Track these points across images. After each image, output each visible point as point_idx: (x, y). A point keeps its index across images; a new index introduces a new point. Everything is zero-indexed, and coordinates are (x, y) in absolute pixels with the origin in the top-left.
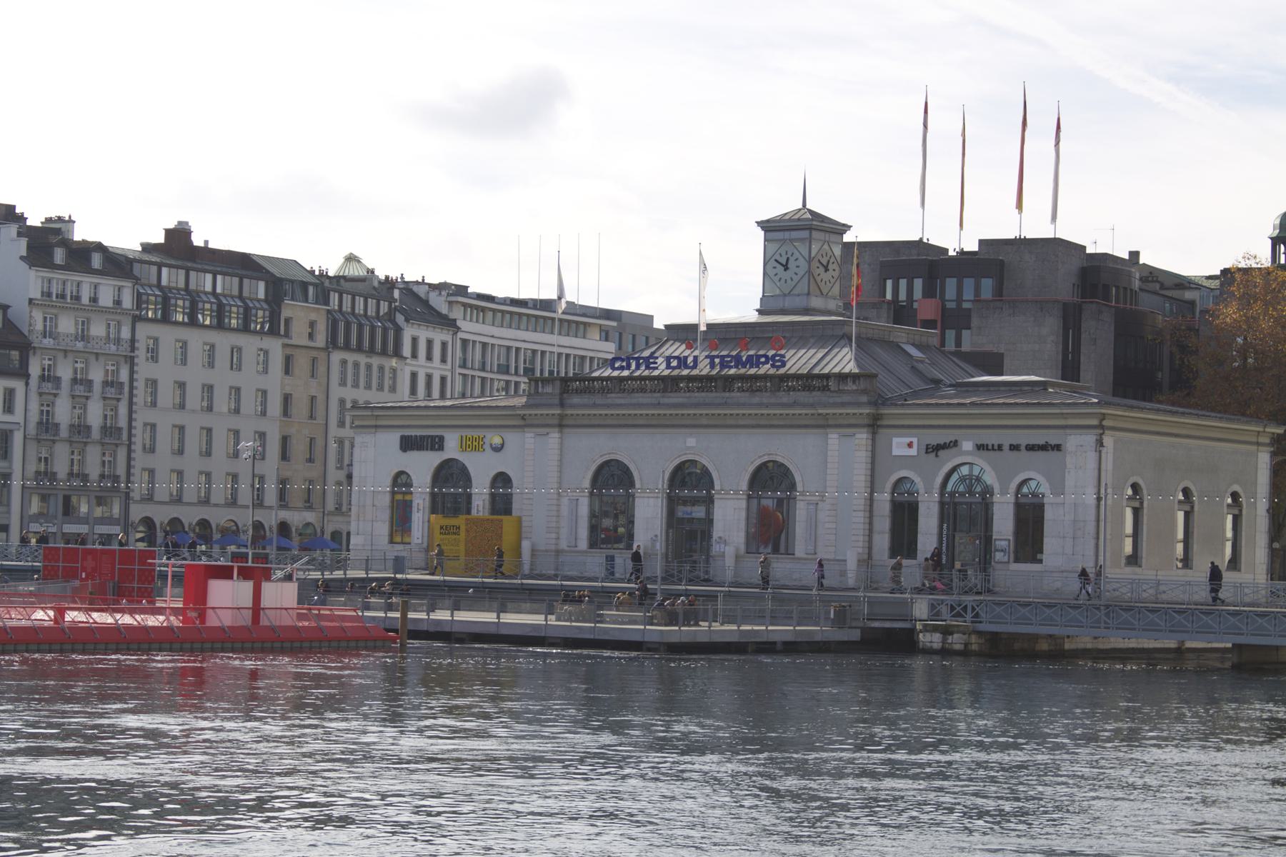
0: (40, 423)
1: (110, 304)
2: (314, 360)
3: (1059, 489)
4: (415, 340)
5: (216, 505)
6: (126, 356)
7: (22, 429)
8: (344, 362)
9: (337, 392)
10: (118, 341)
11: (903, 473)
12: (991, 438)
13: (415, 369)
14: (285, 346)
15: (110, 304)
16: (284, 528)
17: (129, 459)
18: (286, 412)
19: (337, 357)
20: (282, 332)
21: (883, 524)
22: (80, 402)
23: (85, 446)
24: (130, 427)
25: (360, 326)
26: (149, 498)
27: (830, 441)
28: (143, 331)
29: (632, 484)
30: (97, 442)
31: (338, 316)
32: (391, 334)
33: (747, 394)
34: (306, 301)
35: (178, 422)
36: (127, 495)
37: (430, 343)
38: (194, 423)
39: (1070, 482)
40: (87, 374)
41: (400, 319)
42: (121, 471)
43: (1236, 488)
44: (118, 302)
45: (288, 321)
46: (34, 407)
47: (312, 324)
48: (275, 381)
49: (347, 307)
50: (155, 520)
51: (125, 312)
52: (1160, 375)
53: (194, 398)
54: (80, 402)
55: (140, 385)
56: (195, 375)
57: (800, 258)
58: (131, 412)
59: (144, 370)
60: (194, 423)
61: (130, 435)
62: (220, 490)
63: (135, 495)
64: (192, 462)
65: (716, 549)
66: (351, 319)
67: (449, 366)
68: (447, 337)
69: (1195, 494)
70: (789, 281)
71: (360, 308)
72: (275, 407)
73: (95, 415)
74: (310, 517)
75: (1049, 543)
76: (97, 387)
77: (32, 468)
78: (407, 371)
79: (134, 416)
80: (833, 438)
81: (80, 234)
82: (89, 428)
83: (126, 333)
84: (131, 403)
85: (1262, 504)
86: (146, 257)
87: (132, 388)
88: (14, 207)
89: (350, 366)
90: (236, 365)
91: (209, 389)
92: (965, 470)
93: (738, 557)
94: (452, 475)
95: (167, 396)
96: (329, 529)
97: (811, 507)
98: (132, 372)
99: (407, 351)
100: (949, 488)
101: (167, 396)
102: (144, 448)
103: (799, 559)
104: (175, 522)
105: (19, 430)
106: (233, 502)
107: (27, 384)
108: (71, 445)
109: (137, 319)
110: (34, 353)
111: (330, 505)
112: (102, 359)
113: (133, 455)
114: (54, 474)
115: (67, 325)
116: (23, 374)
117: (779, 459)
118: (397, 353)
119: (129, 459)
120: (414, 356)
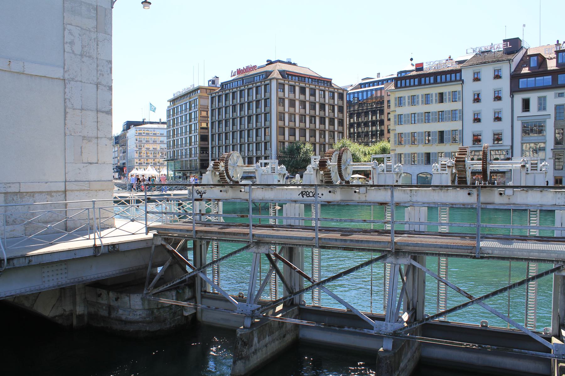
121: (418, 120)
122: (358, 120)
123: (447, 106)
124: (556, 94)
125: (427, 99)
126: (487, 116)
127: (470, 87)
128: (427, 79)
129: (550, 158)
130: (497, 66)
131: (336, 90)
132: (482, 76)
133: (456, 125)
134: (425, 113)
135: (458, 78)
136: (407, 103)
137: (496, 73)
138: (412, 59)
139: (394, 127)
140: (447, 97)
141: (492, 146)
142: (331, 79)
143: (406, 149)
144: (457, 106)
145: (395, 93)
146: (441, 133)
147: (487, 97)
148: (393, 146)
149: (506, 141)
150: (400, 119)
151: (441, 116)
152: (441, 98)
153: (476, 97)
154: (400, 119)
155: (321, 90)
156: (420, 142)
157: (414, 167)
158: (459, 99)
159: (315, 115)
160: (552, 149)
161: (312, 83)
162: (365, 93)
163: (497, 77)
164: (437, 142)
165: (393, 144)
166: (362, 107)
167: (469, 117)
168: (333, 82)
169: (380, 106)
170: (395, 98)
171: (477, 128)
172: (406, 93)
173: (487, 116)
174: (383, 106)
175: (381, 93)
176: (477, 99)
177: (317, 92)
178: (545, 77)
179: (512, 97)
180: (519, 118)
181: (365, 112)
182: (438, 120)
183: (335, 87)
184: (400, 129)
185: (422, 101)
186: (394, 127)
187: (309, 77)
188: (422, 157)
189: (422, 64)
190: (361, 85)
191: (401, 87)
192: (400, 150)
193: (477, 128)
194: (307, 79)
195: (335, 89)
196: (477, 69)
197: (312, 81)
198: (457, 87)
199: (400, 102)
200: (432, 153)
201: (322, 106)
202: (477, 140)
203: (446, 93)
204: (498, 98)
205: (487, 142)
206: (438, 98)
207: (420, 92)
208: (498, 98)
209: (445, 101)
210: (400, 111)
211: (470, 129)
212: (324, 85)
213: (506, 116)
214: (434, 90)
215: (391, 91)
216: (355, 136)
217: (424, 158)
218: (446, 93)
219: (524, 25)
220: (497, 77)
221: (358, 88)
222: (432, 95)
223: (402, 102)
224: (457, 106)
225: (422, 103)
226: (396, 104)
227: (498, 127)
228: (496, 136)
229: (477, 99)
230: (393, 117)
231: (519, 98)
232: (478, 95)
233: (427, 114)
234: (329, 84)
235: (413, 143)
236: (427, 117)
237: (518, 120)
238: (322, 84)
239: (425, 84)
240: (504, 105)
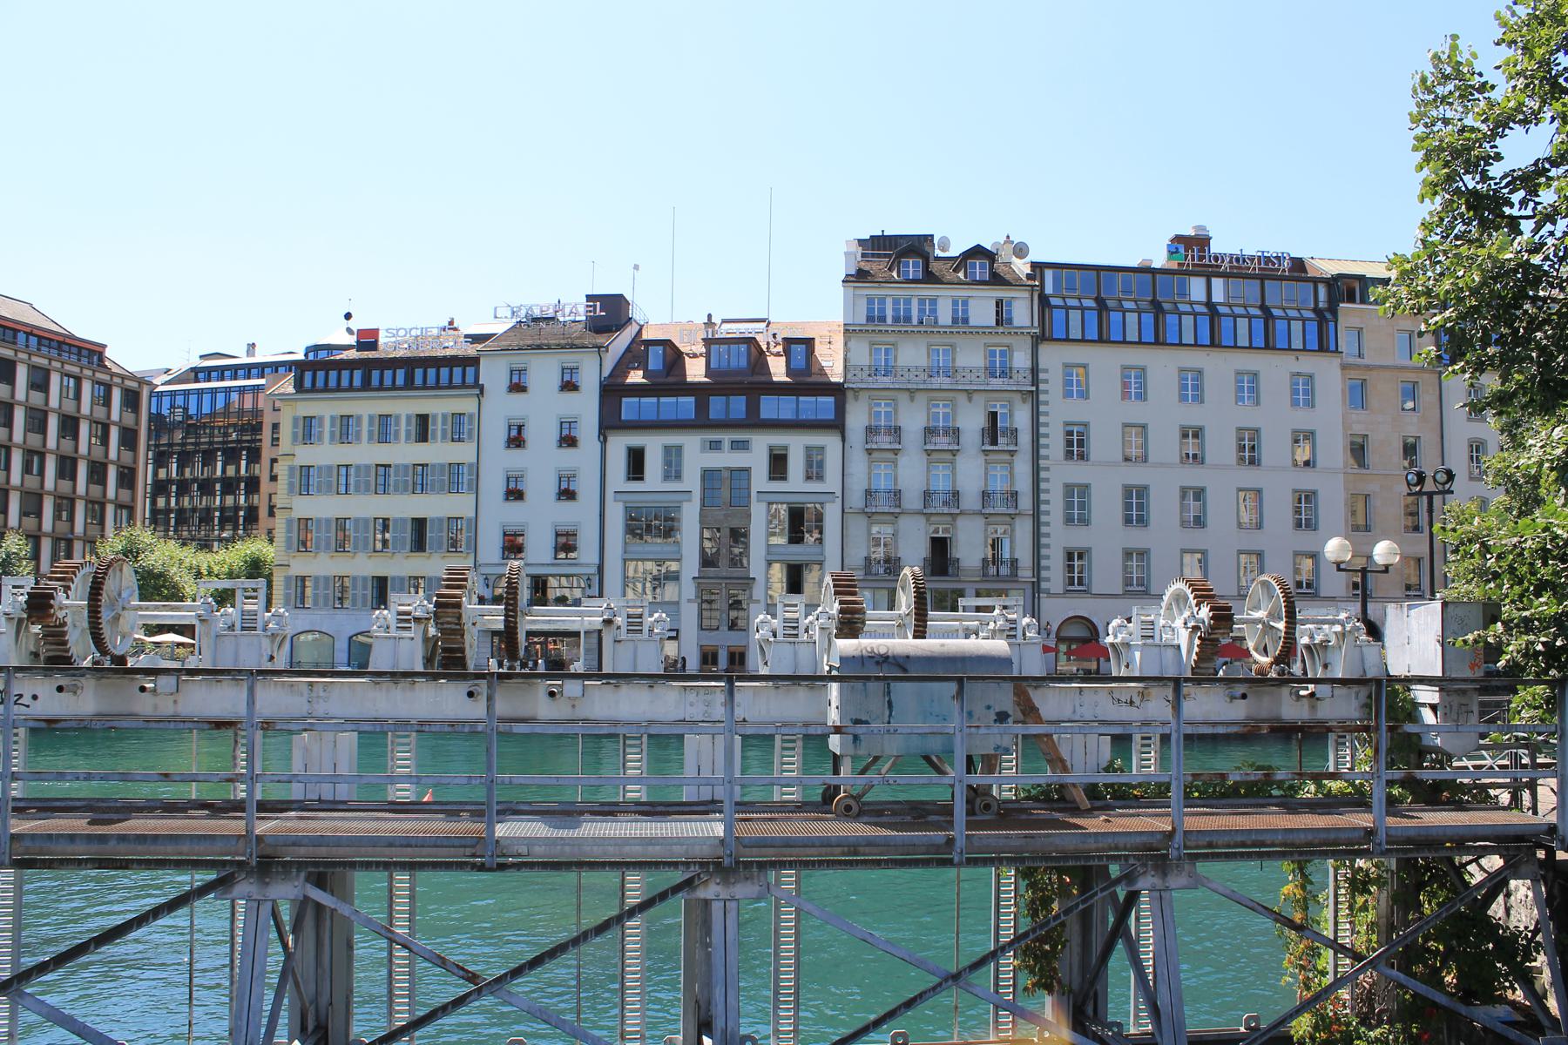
7: (839, 501)
10: (1006, 373)
17: (1037, 535)
23: (954, 520)
28: (1051, 357)
30: (975, 513)
40: (954, 420)
61: (1037, 502)
77: (857, 554)
83: (1021, 360)
105: (834, 502)
108: (928, 520)
109: (1042, 337)
110: (856, 398)
112: (976, 397)
115: (912, 355)
116: (837, 425)
119: (1037, 535)
121: (357, 482)
122: (183, 474)
123: (437, 452)
124: (704, 441)
125: (384, 429)
126: (541, 487)
127: (498, 408)
128: (388, 374)
130: (570, 358)
131: (117, 380)
132: (532, 380)
133: (455, 505)
134: (377, 465)
135: (470, 379)
136: (327, 436)
137: (567, 378)
138: (348, 316)
139: (287, 501)
140: (436, 427)
141: (553, 565)
142: (104, 346)
143: (322, 565)
144: (463, 453)
145: (294, 403)
146: (420, 525)
147: (543, 433)
148: (283, 553)
149: (587, 553)
150: (305, 479)
151: (420, 478)
152: (423, 428)
153: (514, 433)
154: (305, 479)
155: (69, 376)
156: (361, 545)
157: (340, 616)
158: (470, 436)
159: (43, 450)
160: (694, 578)
161: (39, 349)
162: (207, 398)
163: (569, 386)
164: (408, 547)
165: (283, 549)
166: (196, 438)
167: (493, 485)
168: (108, 353)
169: (249, 438)
170: (296, 420)
171: (514, 514)
172: (326, 409)
173: (541, 487)
174: (258, 437)
175: (255, 400)
176: (516, 440)
177: (55, 379)
178: (681, 399)
179: (604, 442)
181: (204, 452)
182: (410, 488)
183: (115, 369)
184: (305, 507)
185: (370, 433)
186: (287, 501)
187: (29, 330)
188: (365, 588)
189: (377, 331)
190: (196, 373)
191: (313, 389)
192: (302, 565)
193: (514, 514)
194: (21, 337)
195: (113, 375)
196: (518, 360)
197: (39, 343)
198: (466, 405)
199: (308, 430)
200: (393, 578)
201: (69, 425)
202: (513, 545)
203: (435, 416)
204: (569, 441)
205: (539, 550)
206: (413, 428)
207: (366, 407)
208: (569, 441)
209: (434, 437)
210: (307, 455)
211: (496, 516)
212: (79, 360)
213: (587, 488)
214: (405, 407)
215: (285, 398)
216: (169, 519)
217: (369, 592)
218: (435, 416)
219: (636, 267)
220: (569, 386)
221: (187, 381)
222: (398, 418)
223: (315, 430)
224: (463, 453)
225: (370, 438)
226: (295, 435)
227: (566, 514)
228: (562, 540)
229: (516, 440)
230: (286, 473)
231: (619, 444)
232: (520, 428)
233: (381, 470)
234: (95, 359)
235: (341, 547)
236: (382, 478)
237: (615, 501)
238: (74, 358)
239: (381, 388)
240: (584, 459)
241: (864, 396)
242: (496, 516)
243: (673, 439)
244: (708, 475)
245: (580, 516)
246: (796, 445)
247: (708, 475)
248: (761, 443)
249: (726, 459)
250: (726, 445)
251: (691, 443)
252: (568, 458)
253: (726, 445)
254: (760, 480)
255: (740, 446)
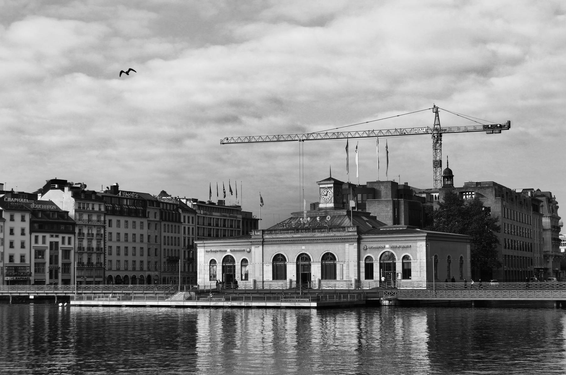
0: (79, 247)
1: (98, 210)
2: (156, 224)
3: (415, 259)
4: (184, 217)
5: (130, 271)
6: (103, 226)
8: (165, 225)
9: (163, 234)
11: (369, 255)
12: (394, 244)
13: (185, 226)
14: (148, 221)
15: (98, 210)
16: (149, 276)
17: (105, 257)
18: (149, 241)
19: (163, 223)
20: (147, 216)
21: (363, 270)
22: (90, 241)
24: (105, 248)
25: (166, 213)
26: (110, 269)
27: (346, 246)
29: (286, 260)
31: (162, 210)
32: (178, 215)
33: (320, 233)
34: (154, 206)
35: (134, 246)
36: (104, 268)
37: (189, 217)
38: (122, 245)
39: (418, 255)
41: (180, 211)
42: (102, 261)
43: (462, 255)
44: (100, 209)
45: (149, 212)
46: (77, 242)
47: (155, 213)
48: (145, 231)
49: (165, 208)
50: (113, 276)
51: (102, 212)
52: (421, 221)
53: (130, 238)
54: (90, 241)
55: (107, 234)
56: (123, 231)
57: (331, 192)
58: (105, 243)
59: (108, 230)
60: (122, 245)
61: (105, 250)
62: (122, 267)
63: (107, 269)
64: (122, 258)
65: (313, 279)
66: (166, 211)
67: (194, 225)
68: (193, 216)
69: (464, 258)
70: (327, 199)
71: (168, 208)
72: (145, 239)
73: (94, 244)
74: (157, 273)
75: (413, 273)
76: (95, 235)
78: (183, 226)
79: (106, 244)
80: (347, 245)
81: (88, 188)
82: (93, 248)
83: (102, 219)
84: (105, 240)
85: (469, 260)
86: (106, 195)
87: (105, 235)
88: (67, 181)
89: (167, 226)
90: (118, 225)
91: (118, 234)
92: (387, 253)
93: (320, 281)
94: (229, 260)
95: (114, 237)
96: (162, 276)
97: (341, 265)
98: (105, 231)
99: (182, 220)
100: (382, 258)
101: (114, 237)
102: (109, 254)
103: (338, 281)
104: (118, 276)
106: (126, 270)
107: (75, 236)
111: (162, 270)
113: (106, 256)
114: (83, 263)
116: (74, 233)
117: (331, 252)
118: (180, 222)
119: (105, 257)
120: (184, 222)
124: (50, 235)
126: (17, 244)
129: (48, 272)
147: (17, 232)
149: (27, 262)
173: (17, 244)
176: (12, 232)
179: (31, 234)
180: (34, 248)
193: (11, 251)
202: (11, 258)
205: (17, 261)
208: (23, 234)
213: (27, 245)
227: (23, 251)
229: (12, 232)
231: (33, 235)
237: (33, 249)
241: (78, 226)
242: (8, 251)
243: (44, 234)
244: (51, 243)
245: (26, 251)
246: (67, 236)
247: (51, 243)
248: (61, 236)
249: (54, 239)
250: (54, 236)
251: (48, 235)
252: (23, 238)
253: (54, 236)
254: (60, 245)
255: (57, 236)
